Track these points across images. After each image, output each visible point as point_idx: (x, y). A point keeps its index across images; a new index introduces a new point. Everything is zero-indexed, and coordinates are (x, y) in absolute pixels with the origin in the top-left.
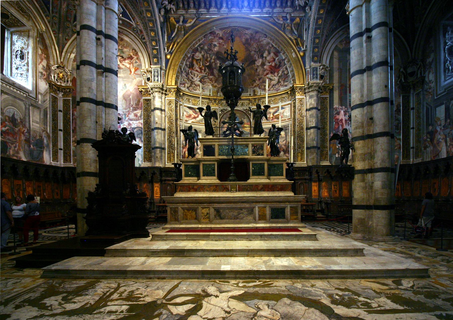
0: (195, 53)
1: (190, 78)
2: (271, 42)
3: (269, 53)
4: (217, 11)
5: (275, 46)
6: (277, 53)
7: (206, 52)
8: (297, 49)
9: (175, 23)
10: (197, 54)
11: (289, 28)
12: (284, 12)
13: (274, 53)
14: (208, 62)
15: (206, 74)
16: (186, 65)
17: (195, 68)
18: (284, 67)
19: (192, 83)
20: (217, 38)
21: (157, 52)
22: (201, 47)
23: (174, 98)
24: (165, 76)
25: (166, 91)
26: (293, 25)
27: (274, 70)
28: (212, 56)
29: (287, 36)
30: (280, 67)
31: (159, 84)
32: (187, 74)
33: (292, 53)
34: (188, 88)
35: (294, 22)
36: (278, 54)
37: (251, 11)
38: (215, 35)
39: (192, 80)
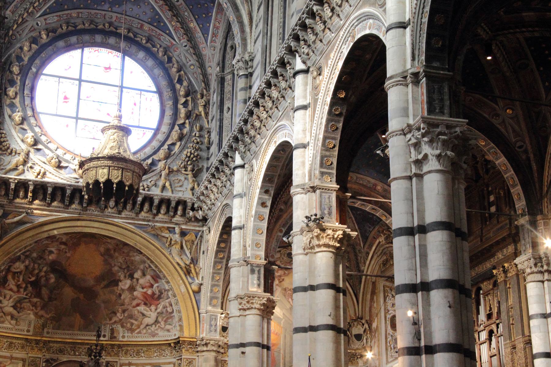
0: (14, 263)
4: (63, 208)
5: (154, 268)
6: (156, 278)
7: (34, 261)
10: (17, 264)
14: (33, 277)
15: (26, 295)
17: (9, 285)
18: (167, 301)
20: (58, 243)
22: (26, 254)
28: (43, 267)
30: (161, 298)
36: (159, 280)
38: (54, 240)
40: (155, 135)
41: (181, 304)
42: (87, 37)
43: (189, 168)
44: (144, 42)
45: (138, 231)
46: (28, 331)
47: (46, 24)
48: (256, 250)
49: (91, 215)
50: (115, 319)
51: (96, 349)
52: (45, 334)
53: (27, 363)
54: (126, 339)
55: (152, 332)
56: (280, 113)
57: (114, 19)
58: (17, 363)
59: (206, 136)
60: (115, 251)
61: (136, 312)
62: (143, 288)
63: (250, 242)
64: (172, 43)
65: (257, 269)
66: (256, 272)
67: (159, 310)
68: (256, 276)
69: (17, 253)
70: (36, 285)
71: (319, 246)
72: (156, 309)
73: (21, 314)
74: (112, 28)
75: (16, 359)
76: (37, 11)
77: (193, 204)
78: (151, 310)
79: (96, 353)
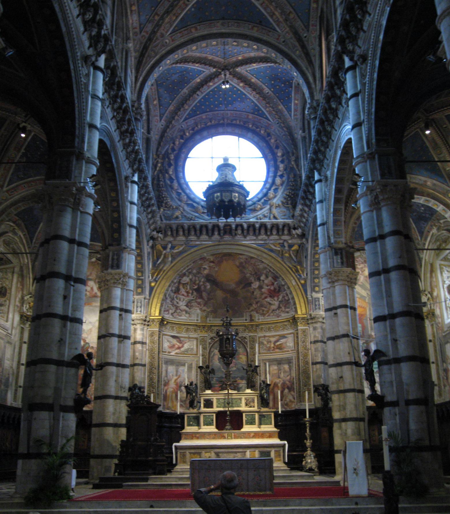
0: (182, 278)
1: (175, 303)
2: (268, 267)
3: (267, 277)
8: (296, 276)
9: (162, 250)
11: (287, 255)
12: (280, 239)
13: (272, 278)
16: (172, 290)
19: (177, 308)
21: (142, 281)
23: (158, 329)
24: (148, 305)
25: (149, 322)
26: (291, 252)
27: (274, 293)
29: (285, 264)
31: (142, 316)
32: (172, 299)
33: (291, 281)
34: (172, 314)
35: (293, 248)
36: (277, 279)
37: (245, 238)
39: (178, 305)
40: (265, 185)
41: (294, 293)
42: (213, 131)
43: (289, 202)
44: (250, 126)
45: (259, 248)
46: (197, 320)
47: (187, 126)
48: (337, 238)
49: (226, 241)
50: (252, 308)
51: (227, 320)
52: (208, 322)
53: (199, 340)
54: (260, 321)
55: (277, 314)
56: (340, 120)
57: (229, 115)
58: (193, 341)
59: (299, 180)
60: (246, 262)
61: (265, 303)
62: (267, 286)
63: (332, 233)
64: (268, 123)
65: (339, 251)
66: (339, 254)
67: (280, 300)
68: (339, 257)
69: (183, 270)
70: (198, 290)
71: (383, 199)
72: (278, 299)
73: (191, 310)
74: (229, 122)
75: (192, 338)
76: (181, 119)
77: (294, 225)
78: (274, 300)
79: (227, 323)
